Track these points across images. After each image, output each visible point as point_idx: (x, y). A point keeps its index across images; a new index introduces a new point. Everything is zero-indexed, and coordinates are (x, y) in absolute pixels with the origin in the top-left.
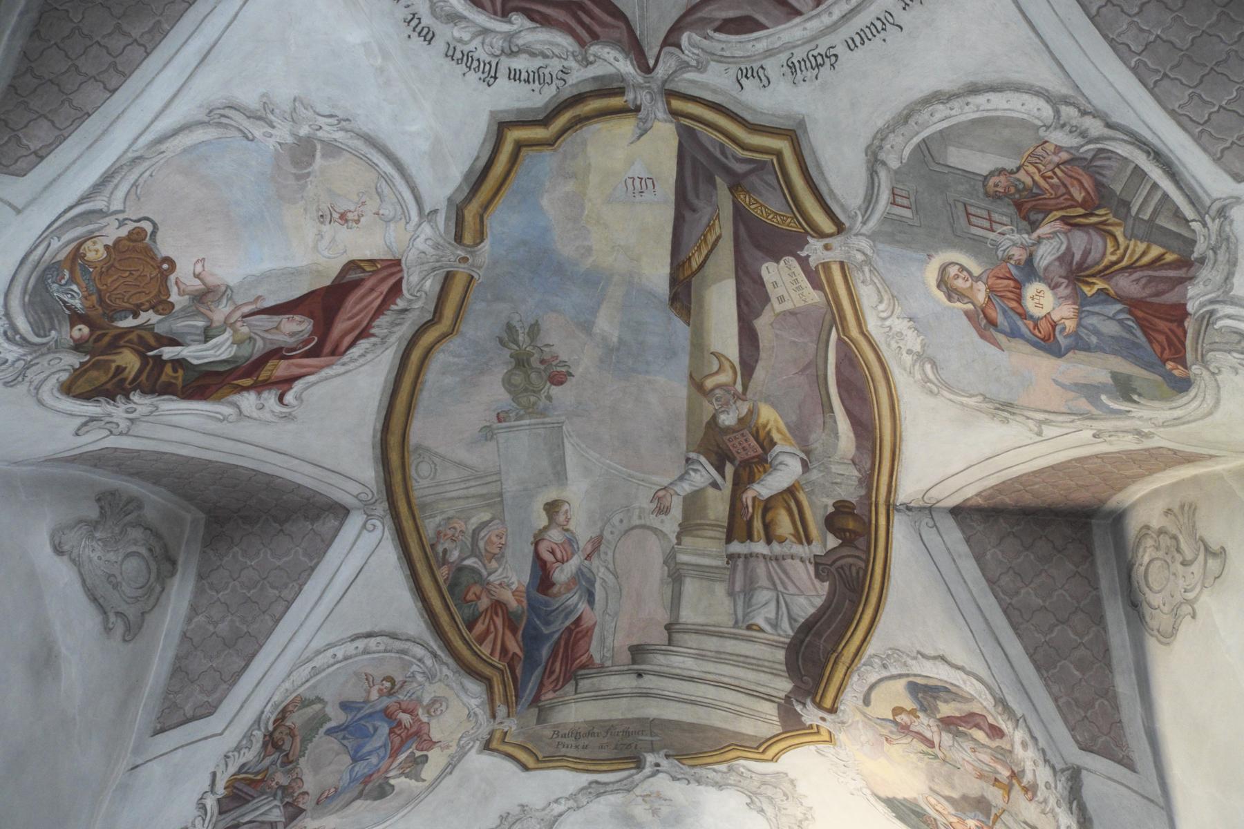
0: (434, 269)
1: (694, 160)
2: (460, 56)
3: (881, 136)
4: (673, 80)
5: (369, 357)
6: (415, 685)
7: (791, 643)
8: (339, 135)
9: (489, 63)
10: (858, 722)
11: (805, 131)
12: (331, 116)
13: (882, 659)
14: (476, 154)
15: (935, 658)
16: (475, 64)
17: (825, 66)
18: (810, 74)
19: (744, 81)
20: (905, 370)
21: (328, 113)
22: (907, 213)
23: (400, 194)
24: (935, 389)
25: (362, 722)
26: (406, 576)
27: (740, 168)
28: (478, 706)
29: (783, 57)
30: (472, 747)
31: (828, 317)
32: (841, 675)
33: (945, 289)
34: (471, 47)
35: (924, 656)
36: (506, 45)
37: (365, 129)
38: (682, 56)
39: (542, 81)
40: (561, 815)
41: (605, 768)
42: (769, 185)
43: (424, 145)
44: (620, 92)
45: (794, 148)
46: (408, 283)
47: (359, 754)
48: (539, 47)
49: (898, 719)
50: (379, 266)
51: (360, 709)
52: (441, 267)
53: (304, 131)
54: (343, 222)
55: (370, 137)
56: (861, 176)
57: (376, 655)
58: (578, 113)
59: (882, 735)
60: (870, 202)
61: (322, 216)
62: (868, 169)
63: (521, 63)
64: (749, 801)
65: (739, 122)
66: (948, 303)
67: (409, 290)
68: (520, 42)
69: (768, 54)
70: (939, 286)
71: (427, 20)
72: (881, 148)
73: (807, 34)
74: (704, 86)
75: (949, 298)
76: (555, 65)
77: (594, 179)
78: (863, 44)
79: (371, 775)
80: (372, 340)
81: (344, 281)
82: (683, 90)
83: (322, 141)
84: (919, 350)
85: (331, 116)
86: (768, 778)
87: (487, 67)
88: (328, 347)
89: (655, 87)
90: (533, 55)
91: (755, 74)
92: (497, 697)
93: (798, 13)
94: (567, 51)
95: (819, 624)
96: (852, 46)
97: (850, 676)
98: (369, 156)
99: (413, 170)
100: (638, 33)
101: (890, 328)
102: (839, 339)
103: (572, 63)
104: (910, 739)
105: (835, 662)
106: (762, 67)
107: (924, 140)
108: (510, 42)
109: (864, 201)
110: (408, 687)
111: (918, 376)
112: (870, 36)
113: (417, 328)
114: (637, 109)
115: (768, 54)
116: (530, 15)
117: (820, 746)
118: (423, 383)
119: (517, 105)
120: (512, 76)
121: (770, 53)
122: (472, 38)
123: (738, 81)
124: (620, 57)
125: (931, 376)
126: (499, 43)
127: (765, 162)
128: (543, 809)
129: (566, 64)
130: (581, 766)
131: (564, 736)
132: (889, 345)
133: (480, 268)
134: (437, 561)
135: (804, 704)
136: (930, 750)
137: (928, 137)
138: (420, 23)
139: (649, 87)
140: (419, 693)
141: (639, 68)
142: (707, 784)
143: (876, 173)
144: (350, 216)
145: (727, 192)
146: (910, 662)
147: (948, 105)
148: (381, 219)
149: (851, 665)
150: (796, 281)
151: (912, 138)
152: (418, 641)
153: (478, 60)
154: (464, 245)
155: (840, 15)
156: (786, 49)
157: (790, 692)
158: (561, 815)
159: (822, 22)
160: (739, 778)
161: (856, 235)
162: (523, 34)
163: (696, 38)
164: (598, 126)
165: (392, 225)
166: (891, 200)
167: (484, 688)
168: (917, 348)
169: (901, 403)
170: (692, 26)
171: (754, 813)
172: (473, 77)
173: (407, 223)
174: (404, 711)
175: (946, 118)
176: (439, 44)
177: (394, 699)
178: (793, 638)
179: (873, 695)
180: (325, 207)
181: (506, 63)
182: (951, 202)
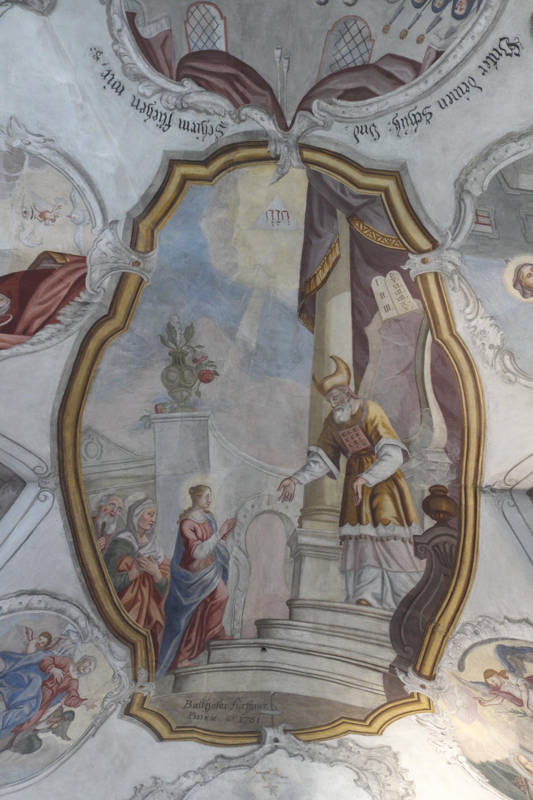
0: (112, 269)
1: (321, 198)
2: (143, 107)
3: (466, 172)
4: (305, 136)
5: (54, 341)
6: (68, 642)
7: (394, 616)
8: (44, 151)
9: (165, 114)
10: (453, 687)
11: (407, 172)
12: (39, 136)
13: (473, 626)
14: (151, 182)
15: (520, 621)
16: (154, 114)
17: (422, 122)
18: (411, 128)
19: (359, 136)
20: (488, 363)
21: (37, 133)
22: (488, 229)
23: (89, 203)
24: (513, 378)
25: (19, 672)
26: (69, 543)
27: (356, 202)
28: (122, 669)
29: (390, 117)
30: (114, 710)
31: (425, 322)
32: (438, 644)
33: (520, 287)
34: (152, 101)
35: (510, 620)
36: (178, 102)
38: (313, 118)
39: (205, 132)
40: (189, 790)
41: (230, 741)
42: (378, 214)
43: (112, 170)
44: (265, 144)
45: (398, 185)
46: (90, 278)
47: (13, 702)
48: (203, 105)
49: (490, 681)
50: (68, 260)
51: (17, 660)
52: (118, 268)
53: (17, 143)
54: (42, 219)
55: (69, 156)
56: (451, 203)
57: (37, 612)
58: (231, 158)
59: (475, 698)
60: (458, 223)
61: (25, 212)
62: (456, 198)
63: (189, 117)
64: (356, 777)
65: (356, 167)
66: (524, 299)
67: (91, 286)
68: (190, 101)
69: (378, 115)
70: (515, 286)
71: (119, 77)
72: (466, 181)
73: (409, 98)
74: (329, 140)
75: (524, 295)
76: (215, 121)
77: (242, 210)
78: (451, 103)
79: (22, 725)
80: (58, 326)
81: (38, 268)
82: (312, 144)
83: (29, 153)
84: (499, 344)
85: (39, 136)
86: (373, 753)
87: (163, 117)
88: (20, 327)
89: (291, 141)
90: (199, 111)
91: (368, 131)
92: (139, 661)
93: (402, 83)
94: (225, 111)
95: (418, 598)
96: (443, 105)
97: (446, 643)
99: (101, 187)
100: (279, 100)
101: (475, 327)
102: (434, 341)
103: (228, 120)
104: (501, 700)
105: (433, 632)
106: (373, 125)
107: (500, 171)
108: (182, 100)
109: (453, 224)
110: (62, 645)
111: (499, 368)
112: (457, 97)
113: (95, 321)
114: (277, 158)
115: (378, 115)
116: (198, 81)
117: (420, 715)
118: (97, 371)
120: (182, 126)
121: (379, 114)
122: (153, 95)
123: (355, 136)
124: (265, 117)
125: (509, 366)
126: (173, 100)
127: (376, 197)
128: (173, 783)
129: (224, 120)
130: (209, 739)
131: (195, 706)
132: (474, 343)
133: (149, 272)
134: (97, 533)
135: (406, 673)
136: (519, 709)
137: (503, 169)
138: (113, 78)
139: (286, 142)
140: (71, 651)
141: (280, 126)
142: (320, 761)
143: (463, 200)
144: (48, 215)
145: (345, 221)
146: (498, 627)
147: (519, 143)
148: (72, 221)
149: (446, 633)
150: (399, 291)
151: (490, 171)
152: (74, 602)
153: (157, 111)
154: (137, 251)
155: (434, 83)
156: (392, 111)
157: (394, 662)
158: (189, 790)
159: (420, 89)
160: (348, 754)
161: (447, 249)
162: (192, 95)
163: (323, 104)
164: (246, 169)
165: (81, 228)
166: (475, 220)
167: (129, 651)
168: (498, 342)
169: (485, 394)
170: (319, 96)
171: (361, 790)
172: (152, 123)
173: (93, 228)
174: (57, 666)
175: (518, 152)
176: (127, 96)
177: (49, 654)
178: (397, 612)
179: (467, 661)
180: (28, 206)
181: (178, 115)
182: (523, 217)
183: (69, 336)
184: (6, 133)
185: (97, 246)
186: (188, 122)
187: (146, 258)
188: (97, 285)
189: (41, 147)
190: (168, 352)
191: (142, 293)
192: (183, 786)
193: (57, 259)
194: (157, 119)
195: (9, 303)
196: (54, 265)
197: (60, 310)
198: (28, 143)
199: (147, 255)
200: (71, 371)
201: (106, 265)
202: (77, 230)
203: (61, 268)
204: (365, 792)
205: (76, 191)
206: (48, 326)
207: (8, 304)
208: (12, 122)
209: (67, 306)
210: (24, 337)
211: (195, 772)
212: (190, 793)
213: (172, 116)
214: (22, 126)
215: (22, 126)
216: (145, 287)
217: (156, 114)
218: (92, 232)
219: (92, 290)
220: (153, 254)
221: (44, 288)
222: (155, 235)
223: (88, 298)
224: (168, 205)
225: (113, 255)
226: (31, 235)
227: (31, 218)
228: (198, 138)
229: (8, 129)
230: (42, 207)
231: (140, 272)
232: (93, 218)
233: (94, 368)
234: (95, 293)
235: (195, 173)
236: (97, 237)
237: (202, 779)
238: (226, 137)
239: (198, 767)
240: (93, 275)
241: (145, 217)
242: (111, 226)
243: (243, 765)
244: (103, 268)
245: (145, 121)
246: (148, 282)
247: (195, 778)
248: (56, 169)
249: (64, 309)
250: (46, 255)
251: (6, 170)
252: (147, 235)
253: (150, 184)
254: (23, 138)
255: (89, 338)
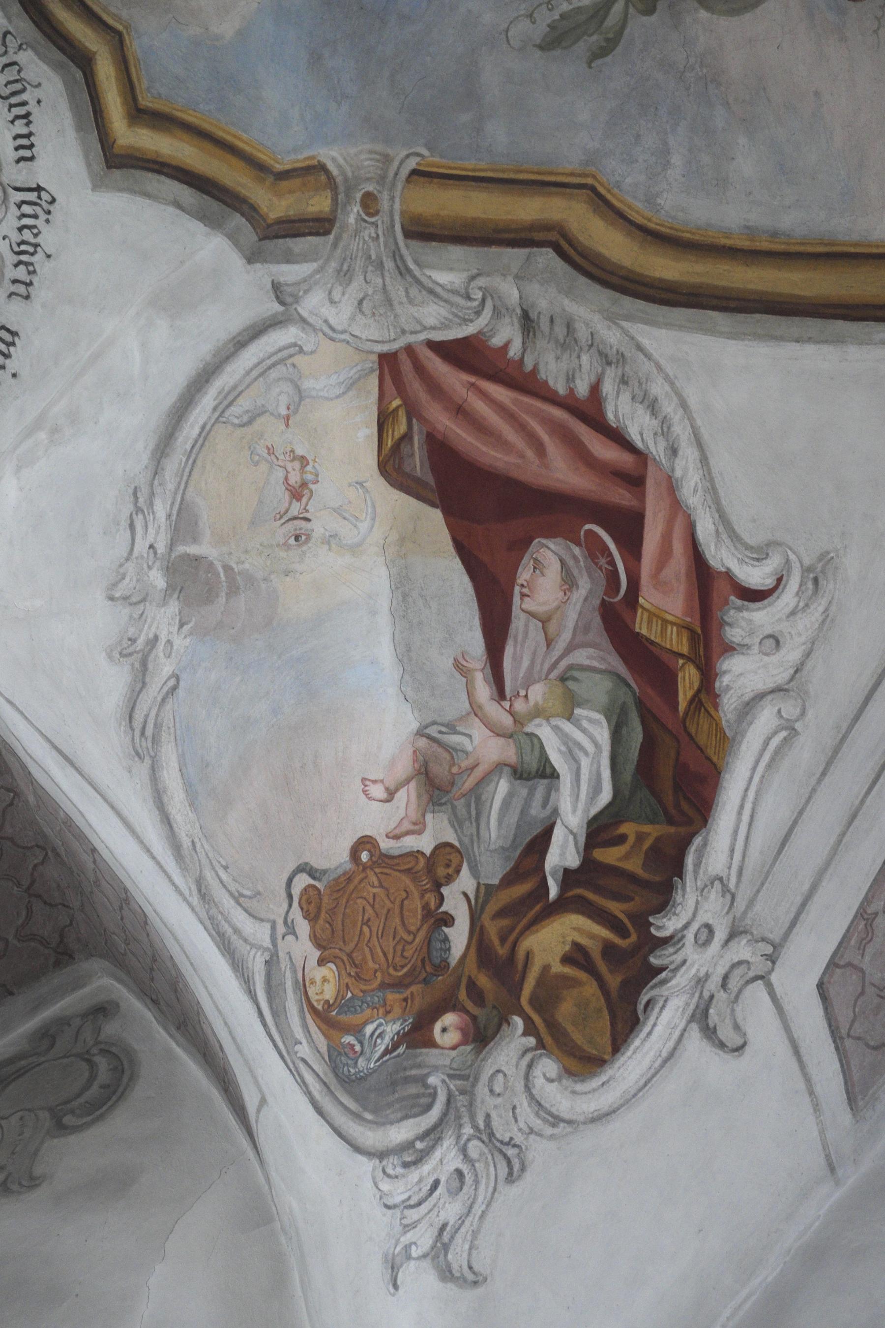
0: (403, 271)
2: (22, 268)
5: (658, 388)
8: (161, 509)
12: (132, 526)
14: (171, 209)
16: (27, 235)
23: (248, 373)
37: (145, 458)
39: (18, 86)
46: (444, 326)
50: (397, 402)
52: (396, 255)
53: (157, 579)
54: (306, 492)
55: (157, 446)
61: (297, 538)
67: (466, 321)
80: (608, 388)
81: (431, 480)
83: (171, 546)
85: (132, 526)
87: (26, 209)
88: (621, 496)
98: (188, 447)
99: (205, 350)
113: (583, 280)
118: (750, 231)
119: (71, 134)
120: (27, 153)
133: (387, 159)
144: (295, 479)
148: (296, 411)
153: (20, 229)
154: (334, 211)
165: (307, 384)
172: (48, 238)
173: (301, 351)
180: (283, 532)
183: (640, 348)
184: (141, 607)
185: (344, 332)
186: (15, 138)
187: (346, 180)
188: (461, 302)
189: (154, 518)
190: (645, 19)
191: (459, 163)
193: (397, 435)
194: (35, 227)
195: (544, 541)
196: (416, 439)
197: (555, 392)
198: (151, 550)
199: (339, 180)
200: (757, 316)
201: (393, 295)
202: (314, 393)
203: (422, 419)
205: (226, 414)
206: (610, 416)
207: (551, 543)
208: (117, 595)
209: (542, 375)
210: (650, 483)
213: (18, 185)
214: (122, 570)
215: (122, 570)
216: (436, 159)
217: (26, 231)
218: (312, 352)
219: (478, 313)
220: (334, 160)
221: (493, 453)
222: (288, 167)
223: (507, 320)
224: (208, 146)
225: (362, 278)
226: (347, 515)
227: (308, 520)
228: (39, 102)
229: (135, 604)
230: (279, 496)
231: (393, 185)
232: (280, 355)
233: (745, 244)
234: (489, 304)
235: (115, 87)
236: (320, 334)
238: (10, 21)
240: (431, 321)
241: (254, 208)
242: (289, 300)
244: (405, 300)
245: (49, 256)
246: (418, 155)
248: (190, 475)
249: (551, 383)
250: (389, 468)
251: (217, 596)
252: (291, 192)
253: (178, 211)
254: (145, 566)
255: (645, 285)
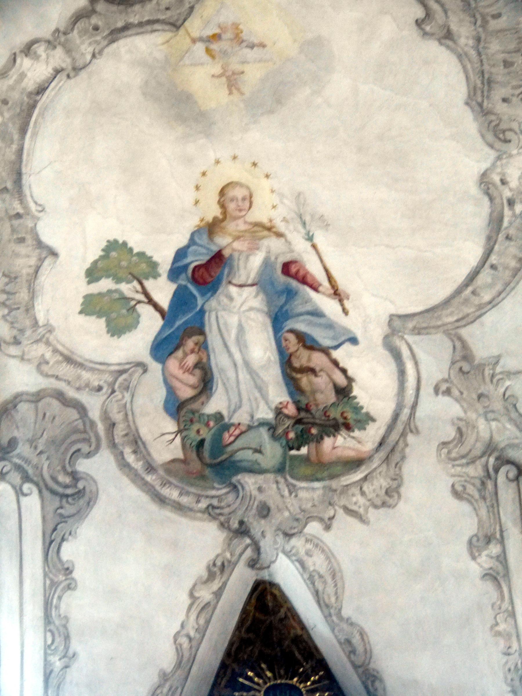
40: (41, 90)
64: (420, 13)
158: (41, 90)
192: (26, 80)
204: (443, 49)
211: (49, 42)
212: (44, 99)
237: (69, 60)
239: (53, 28)
243: (157, 21)
247: (51, 60)
